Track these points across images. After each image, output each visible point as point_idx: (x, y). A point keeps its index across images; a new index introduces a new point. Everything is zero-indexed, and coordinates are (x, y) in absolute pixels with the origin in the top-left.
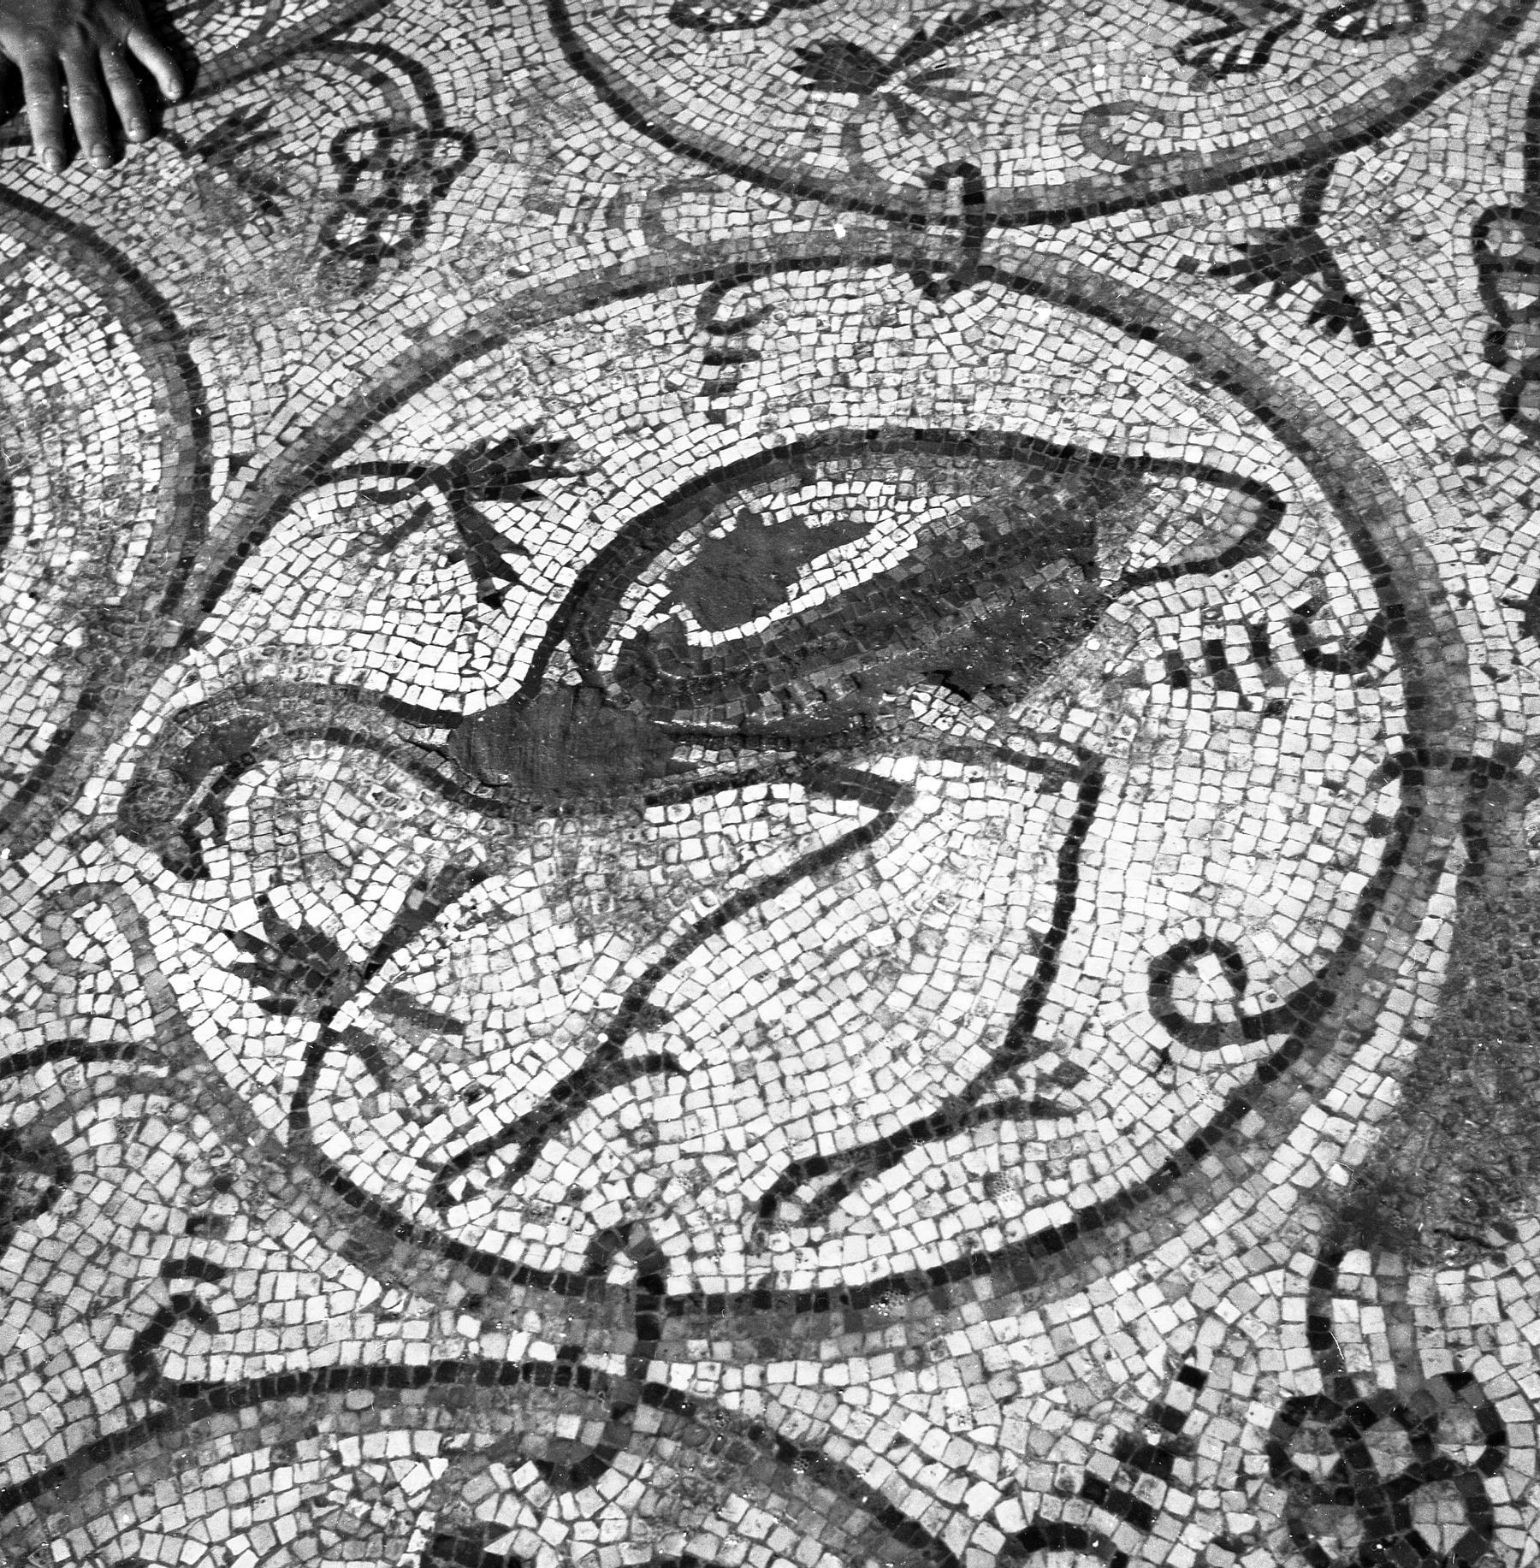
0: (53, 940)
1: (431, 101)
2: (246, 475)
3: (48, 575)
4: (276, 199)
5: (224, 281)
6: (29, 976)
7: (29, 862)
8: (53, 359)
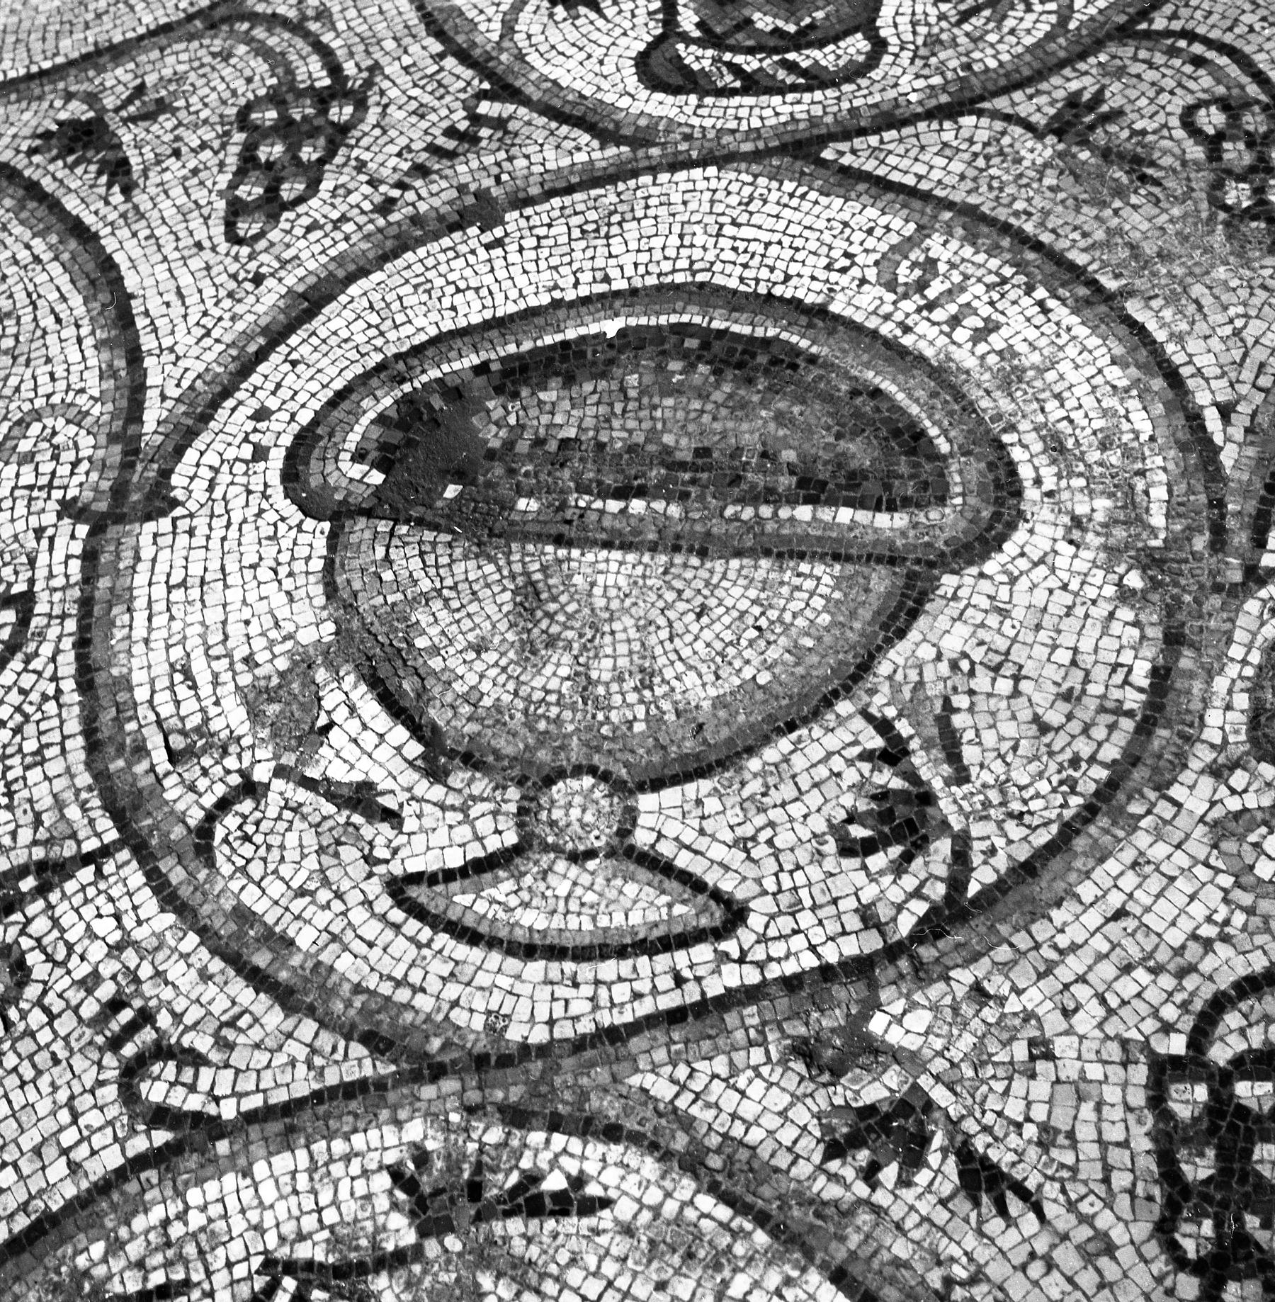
0: (1237, 865)
1: (1259, 77)
2: (1240, 421)
3: (1077, 522)
4: (1150, 171)
5: (1132, 247)
6: (1226, 900)
7: (1176, 792)
8: (991, 327)
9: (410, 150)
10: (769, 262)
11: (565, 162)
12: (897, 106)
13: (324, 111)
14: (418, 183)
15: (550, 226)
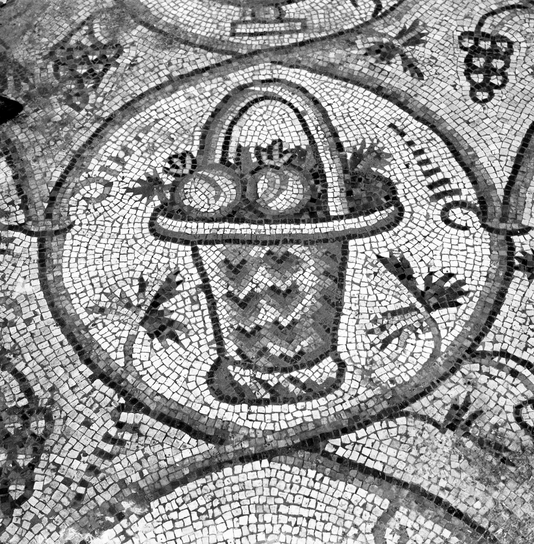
4: (505, 455)
9: (85, 455)
10: (311, 532)
11: (178, 459)
12: (361, 411)
13: (26, 425)
14: (94, 481)
15: (178, 511)
